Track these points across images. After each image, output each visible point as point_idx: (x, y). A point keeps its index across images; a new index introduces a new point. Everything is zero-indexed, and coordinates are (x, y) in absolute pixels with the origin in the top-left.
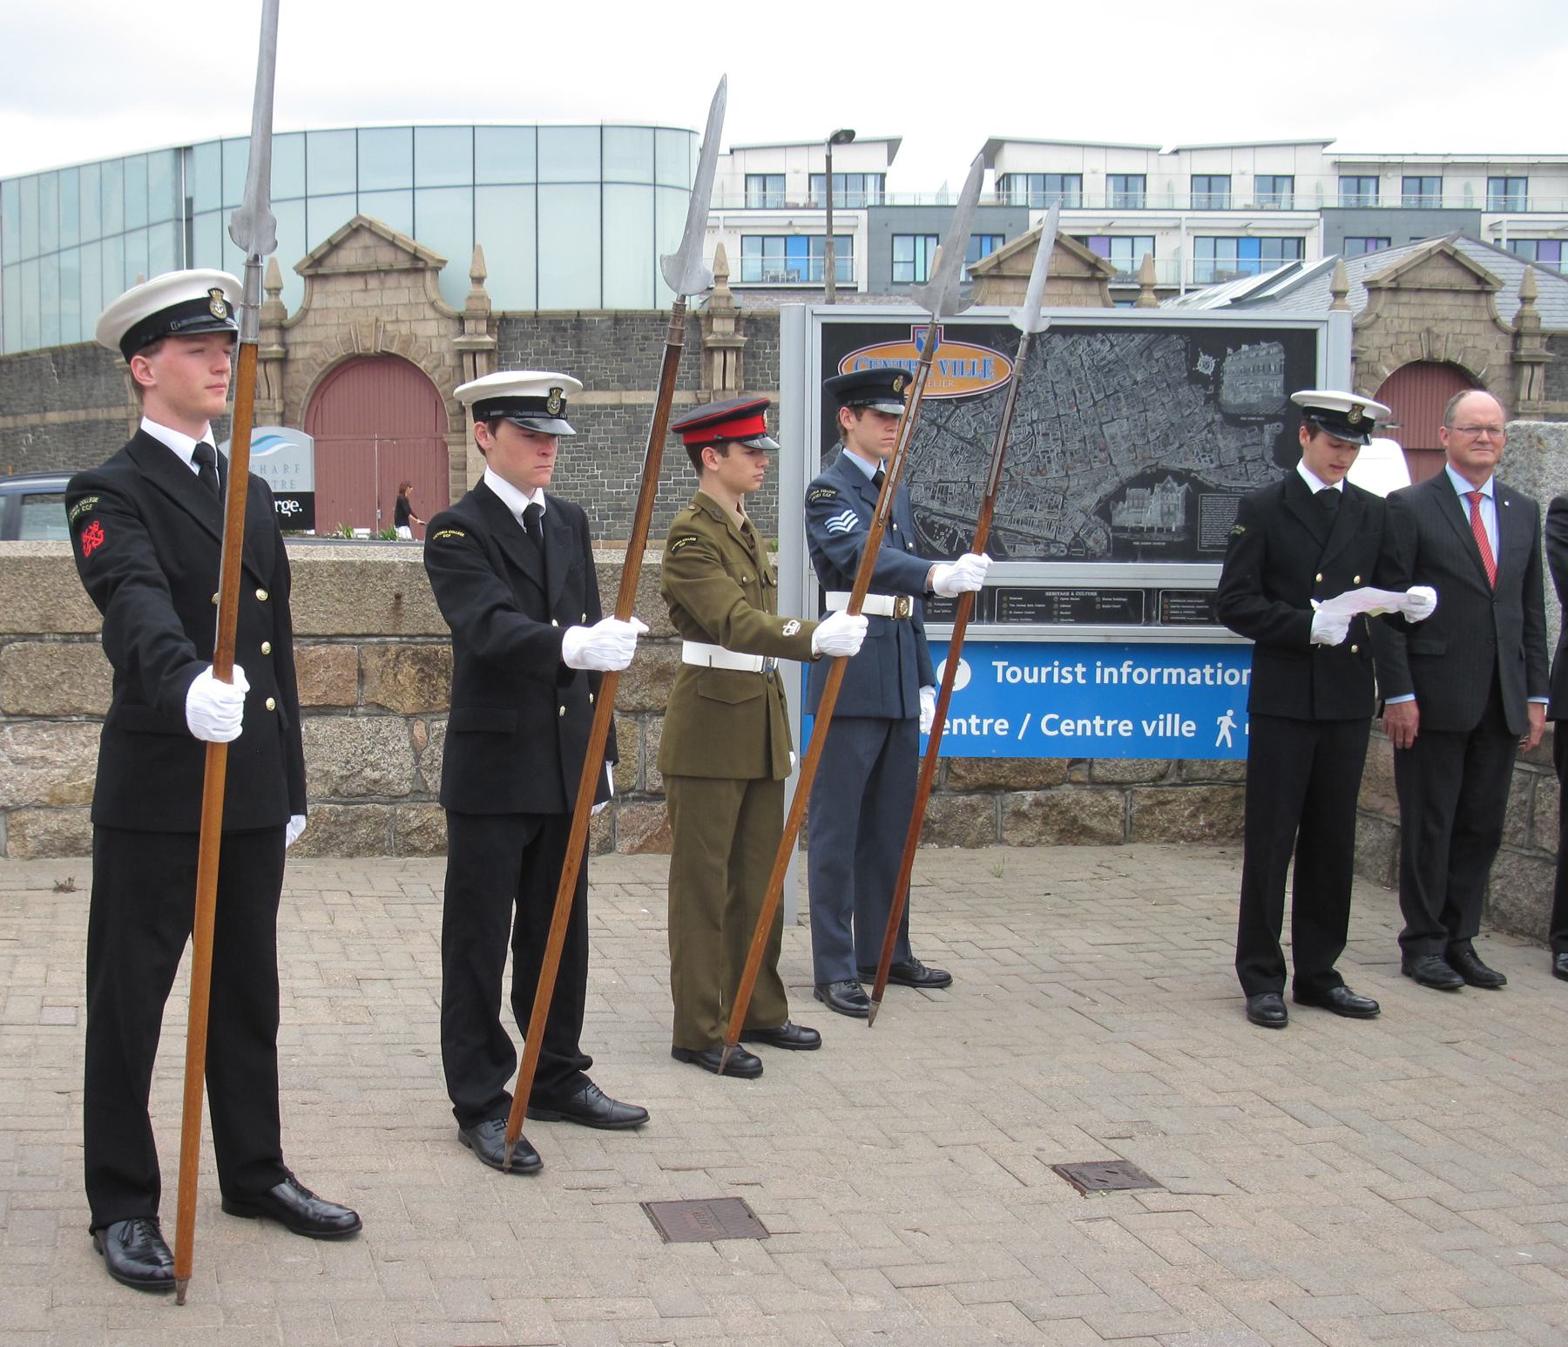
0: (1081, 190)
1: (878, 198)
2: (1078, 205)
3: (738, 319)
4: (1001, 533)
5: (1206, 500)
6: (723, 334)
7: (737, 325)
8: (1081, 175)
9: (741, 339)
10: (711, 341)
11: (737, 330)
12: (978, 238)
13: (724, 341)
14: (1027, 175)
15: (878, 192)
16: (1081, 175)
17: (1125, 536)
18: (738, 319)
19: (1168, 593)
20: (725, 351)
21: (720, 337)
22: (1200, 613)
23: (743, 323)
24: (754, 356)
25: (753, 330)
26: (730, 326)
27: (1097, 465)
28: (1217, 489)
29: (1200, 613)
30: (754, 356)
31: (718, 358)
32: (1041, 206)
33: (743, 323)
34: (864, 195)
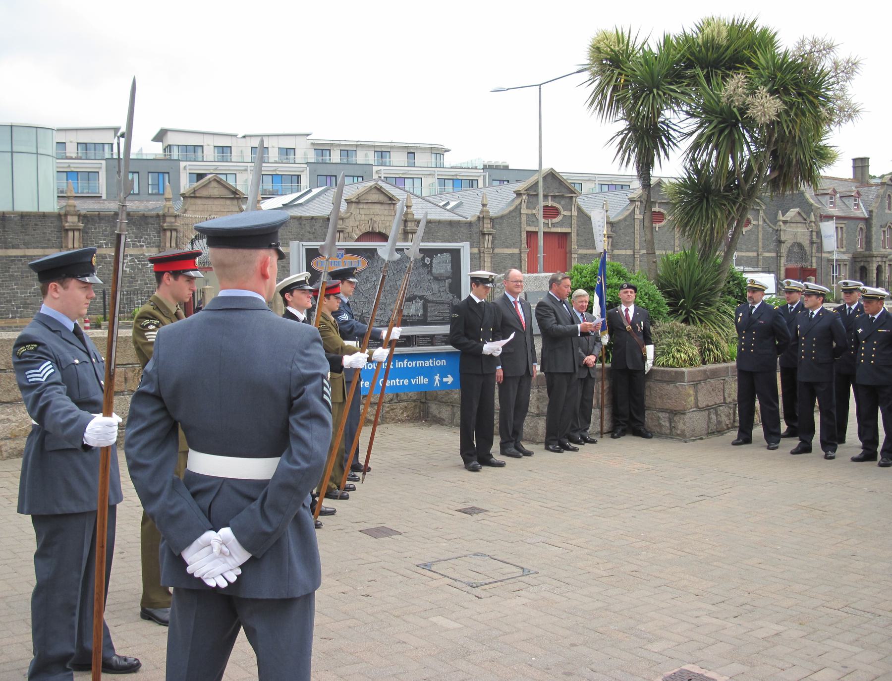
0: (203, 153)
1: (110, 155)
2: (201, 159)
3: (79, 216)
4: (365, 318)
5: (429, 305)
6: (72, 223)
7: (79, 218)
8: (202, 146)
9: (81, 225)
10: (68, 226)
11: (79, 221)
12: (157, 174)
13: (73, 226)
14: (178, 145)
15: (110, 152)
16: (202, 146)
17: (404, 318)
18: (79, 216)
19: (418, 336)
20: (73, 230)
21: (71, 224)
22: (429, 342)
23: (81, 218)
24: (87, 233)
25: (86, 221)
26: (75, 219)
27: (395, 295)
28: (432, 301)
29: (429, 342)
30: (87, 233)
31: (70, 234)
32: (185, 159)
33: (81, 218)
34: (104, 153)
